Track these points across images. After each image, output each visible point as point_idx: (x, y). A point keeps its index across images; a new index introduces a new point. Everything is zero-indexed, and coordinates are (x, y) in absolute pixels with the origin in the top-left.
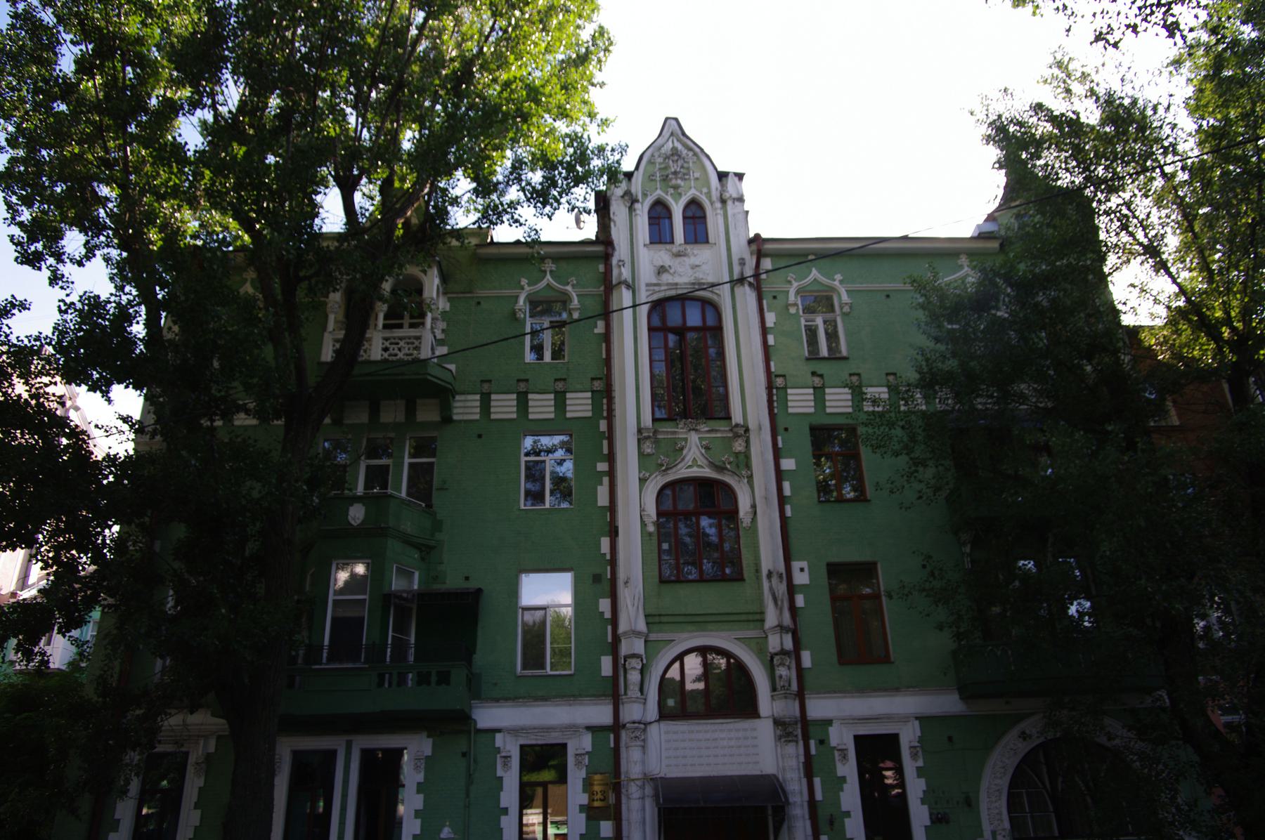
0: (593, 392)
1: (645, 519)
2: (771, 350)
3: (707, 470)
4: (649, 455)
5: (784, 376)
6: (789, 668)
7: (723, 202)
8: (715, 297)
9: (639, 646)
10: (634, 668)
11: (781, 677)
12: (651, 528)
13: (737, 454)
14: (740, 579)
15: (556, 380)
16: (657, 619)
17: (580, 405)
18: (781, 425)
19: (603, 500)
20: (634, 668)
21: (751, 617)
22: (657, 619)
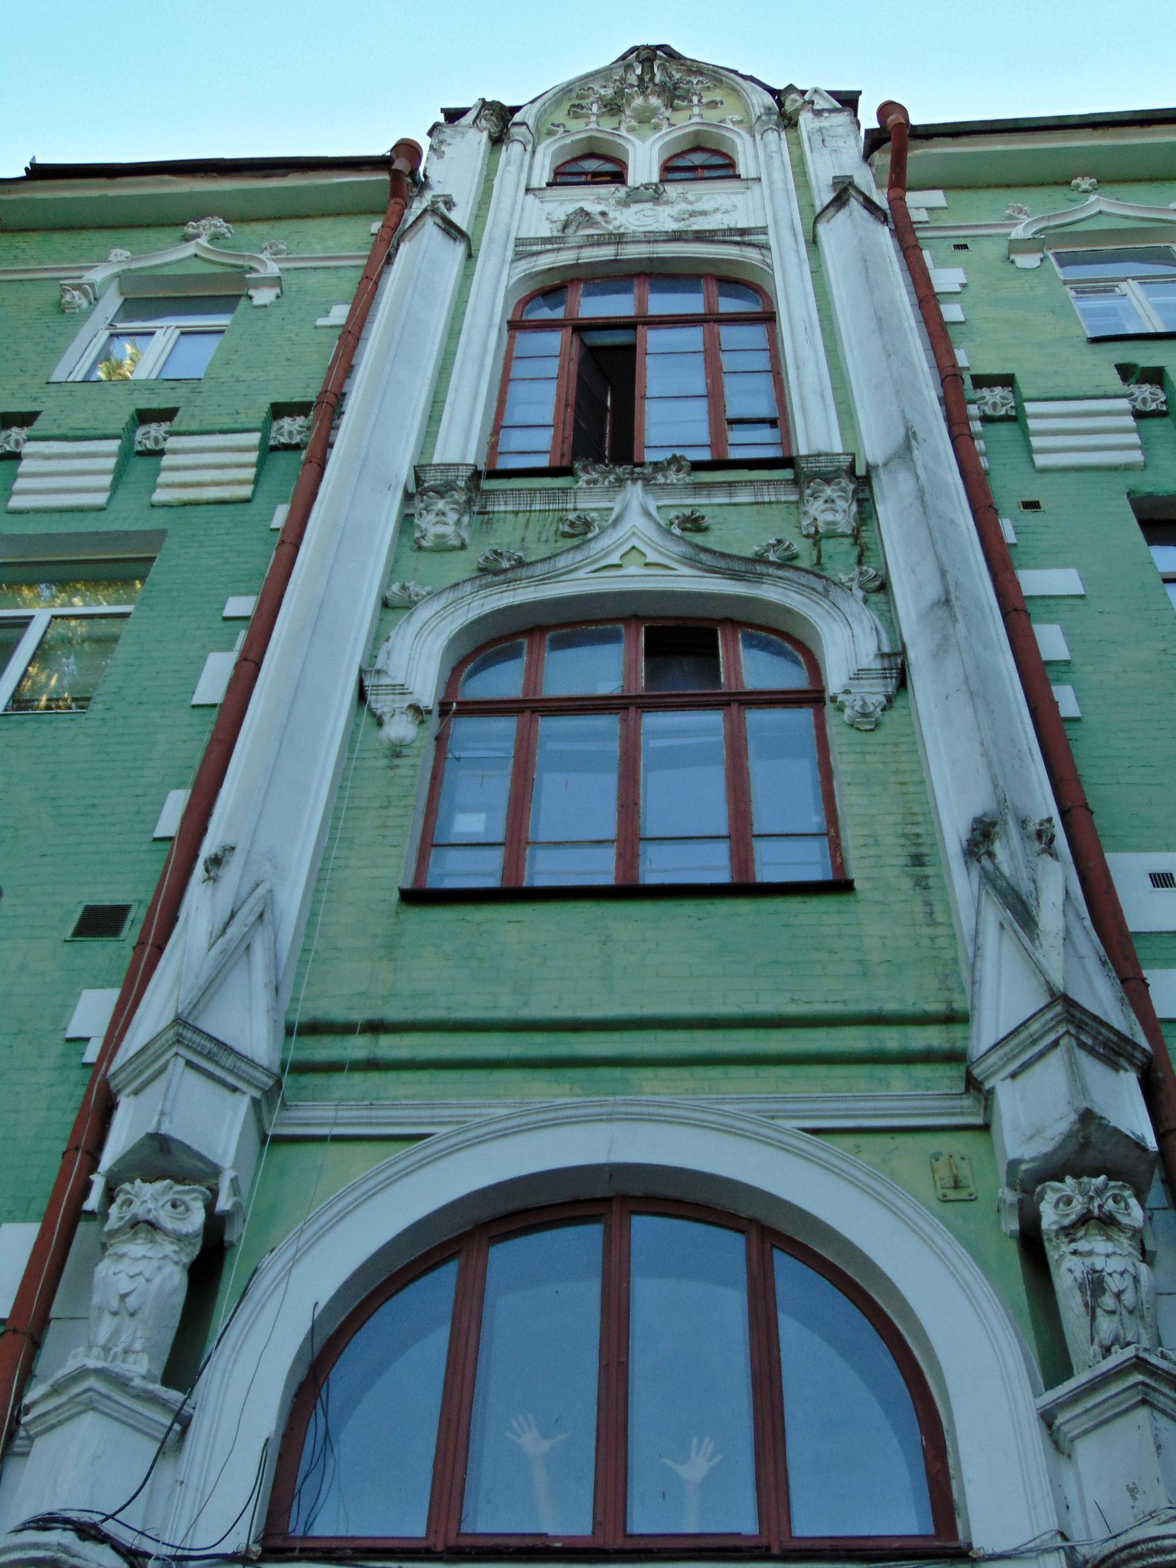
0: (268, 450)
1: (381, 703)
2: (952, 331)
3: (684, 570)
4: (442, 548)
5: (1007, 381)
6: (1146, 1256)
7: (789, 122)
8: (752, 254)
9: (216, 1124)
10: (146, 1226)
11: (1095, 1285)
12: (401, 728)
13: (816, 538)
14: (840, 886)
15: (144, 417)
16: (358, 1047)
17: (209, 465)
18: (1008, 489)
19: (214, 679)
20: (146, 1226)
21: (891, 1039)
22: (358, 1047)
